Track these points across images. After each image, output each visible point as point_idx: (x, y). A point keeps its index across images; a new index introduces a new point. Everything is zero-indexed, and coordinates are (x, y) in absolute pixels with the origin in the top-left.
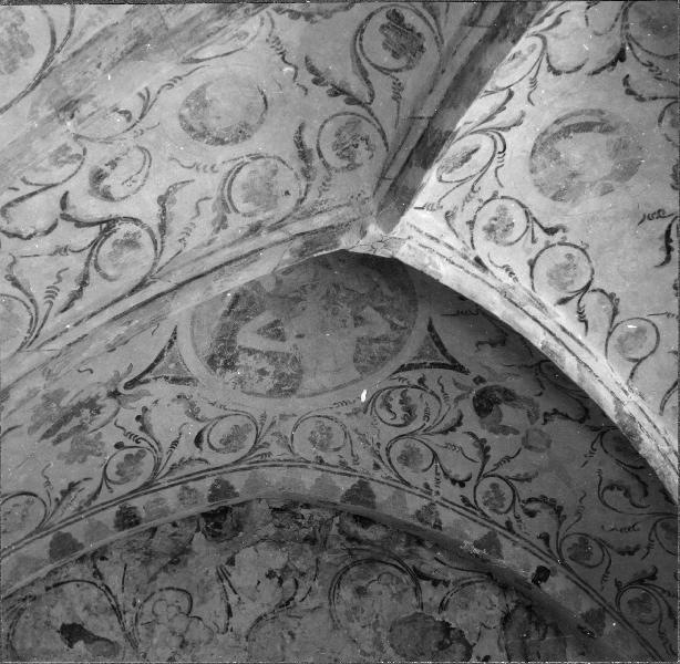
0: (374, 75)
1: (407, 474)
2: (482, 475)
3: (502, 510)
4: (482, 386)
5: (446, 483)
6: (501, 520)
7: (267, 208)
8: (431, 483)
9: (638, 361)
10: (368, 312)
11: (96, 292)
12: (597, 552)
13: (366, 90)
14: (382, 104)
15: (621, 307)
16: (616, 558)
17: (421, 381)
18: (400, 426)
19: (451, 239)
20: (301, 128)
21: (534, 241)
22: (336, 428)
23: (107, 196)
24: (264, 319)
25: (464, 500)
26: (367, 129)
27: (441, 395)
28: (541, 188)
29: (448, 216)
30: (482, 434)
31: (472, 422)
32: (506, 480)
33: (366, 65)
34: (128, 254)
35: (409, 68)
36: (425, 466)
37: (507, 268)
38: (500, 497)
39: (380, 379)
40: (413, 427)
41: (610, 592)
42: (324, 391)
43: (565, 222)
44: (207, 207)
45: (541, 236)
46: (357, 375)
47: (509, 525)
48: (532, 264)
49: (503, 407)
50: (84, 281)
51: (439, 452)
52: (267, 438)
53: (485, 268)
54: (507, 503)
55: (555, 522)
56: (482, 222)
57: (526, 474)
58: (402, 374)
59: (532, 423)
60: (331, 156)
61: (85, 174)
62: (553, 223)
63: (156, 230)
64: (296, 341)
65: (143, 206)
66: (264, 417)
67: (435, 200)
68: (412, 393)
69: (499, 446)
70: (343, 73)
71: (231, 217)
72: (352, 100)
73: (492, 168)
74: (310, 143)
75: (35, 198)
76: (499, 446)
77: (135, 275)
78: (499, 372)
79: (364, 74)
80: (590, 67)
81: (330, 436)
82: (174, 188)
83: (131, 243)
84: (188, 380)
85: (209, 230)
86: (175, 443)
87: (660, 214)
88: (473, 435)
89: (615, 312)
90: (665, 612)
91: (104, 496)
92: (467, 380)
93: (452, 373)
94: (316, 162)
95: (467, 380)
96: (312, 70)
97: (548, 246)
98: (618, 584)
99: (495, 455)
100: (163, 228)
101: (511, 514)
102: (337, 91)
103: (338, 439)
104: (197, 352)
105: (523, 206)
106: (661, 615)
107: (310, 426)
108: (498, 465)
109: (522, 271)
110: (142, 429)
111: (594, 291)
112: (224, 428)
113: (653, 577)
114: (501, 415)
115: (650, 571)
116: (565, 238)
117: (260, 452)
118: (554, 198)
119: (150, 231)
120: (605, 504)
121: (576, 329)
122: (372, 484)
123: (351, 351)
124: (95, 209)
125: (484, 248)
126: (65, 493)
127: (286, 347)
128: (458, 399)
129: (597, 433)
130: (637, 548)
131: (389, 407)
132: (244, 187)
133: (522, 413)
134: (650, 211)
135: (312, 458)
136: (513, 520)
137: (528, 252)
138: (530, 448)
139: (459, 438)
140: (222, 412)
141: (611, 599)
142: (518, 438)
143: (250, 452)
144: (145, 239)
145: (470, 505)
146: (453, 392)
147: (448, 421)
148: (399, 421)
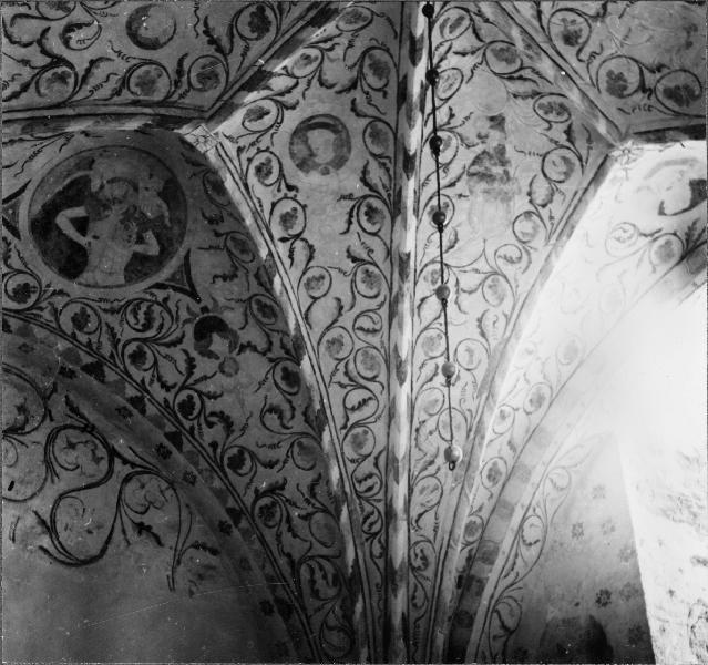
0: (237, 39)
1: (132, 370)
2: (183, 387)
3: (190, 417)
4: (206, 315)
5: (156, 385)
7: (146, 95)
8: (147, 381)
9: (315, 299)
10: (149, 236)
11: (24, 99)
12: (248, 463)
13: (228, 47)
14: (234, 60)
15: (315, 254)
16: (261, 469)
17: (166, 300)
18: (138, 331)
19: (236, 163)
20: (186, 55)
21: (279, 190)
23: (66, 43)
24: (79, 212)
26: (220, 69)
27: (175, 316)
28: (292, 155)
29: (240, 150)
30: (194, 354)
31: (189, 343)
32: (200, 394)
33: (235, 32)
34: (57, 86)
35: (257, 39)
36: (147, 366)
37: (260, 201)
38: (192, 406)
39: (137, 290)
40: (150, 334)
41: (249, 498)
42: (96, 286)
43: (299, 185)
44: (114, 79)
45: (283, 186)
46: (122, 281)
48: (274, 205)
49: (216, 337)
50: (25, 88)
51: (160, 359)
52: (44, 305)
53: (249, 193)
54: (195, 413)
55: (224, 436)
56: (256, 163)
57: (215, 393)
58: (155, 291)
59: (231, 352)
60: (194, 80)
61: (64, 23)
62: (292, 182)
63: (80, 79)
64: (92, 240)
65: (80, 61)
66: (48, 286)
67: (235, 137)
68: (157, 309)
69: (204, 366)
70: (220, 31)
71: (125, 91)
72: (220, 49)
73: (272, 131)
74: (186, 66)
75: (33, 21)
76: (204, 366)
77: (55, 98)
78: (221, 305)
79: (231, 36)
80: (337, 88)
81: (87, 321)
82: (100, 59)
83: (62, 78)
84: (16, 233)
85: (109, 92)
87: (350, 197)
89: (311, 258)
90: (284, 519)
92: (196, 308)
93: (187, 300)
94: (185, 79)
95: (196, 308)
96: (206, 24)
97: (286, 197)
98: (256, 491)
99: (198, 373)
100: (85, 79)
101: (195, 422)
102: (212, 41)
103: (92, 325)
104: (29, 212)
105: (280, 163)
106: (281, 520)
107: (76, 308)
108: (196, 382)
109: (267, 207)
111: (303, 240)
113: (282, 488)
114: (211, 341)
115: (281, 482)
116: (295, 196)
117: (34, 311)
118: (297, 166)
119: (76, 75)
120: (264, 425)
121: (287, 262)
122: (106, 369)
123: (126, 260)
124: (55, 44)
125: (252, 180)
127: (83, 241)
128: (186, 322)
129: (273, 364)
130: (277, 462)
131: (136, 317)
132: (139, 77)
133: (227, 343)
134: (347, 193)
135: (69, 333)
136: (197, 427)
137: (274, 196)
138: (223, 372)
139: (176, 353)
140: (23, 268)
141: (249, 504)
142: (217, 363)
143: (28, 309)
144: (71, 81)
145: (168, 406)
146: (184, 315)
148: (139, 327)
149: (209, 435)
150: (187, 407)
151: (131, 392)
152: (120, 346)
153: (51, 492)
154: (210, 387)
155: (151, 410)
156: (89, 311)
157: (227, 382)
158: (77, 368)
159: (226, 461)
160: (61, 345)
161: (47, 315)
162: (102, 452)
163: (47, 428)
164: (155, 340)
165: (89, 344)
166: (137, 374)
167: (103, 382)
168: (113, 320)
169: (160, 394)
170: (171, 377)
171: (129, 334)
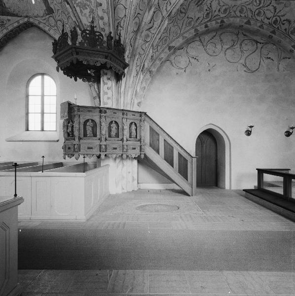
1: (259, 18)
5: (266, 19)
6: (276, 27)
22: (245, 8)
25: (269, 23)
40: (261, 5)
47: (278, 29)
51: (266, 12)
76: (279, 8)
86: (215, 11)
88: (273, 6)
91: (203, 22)
99: (277, 11)
107: (239, 8)
110: (210, 6)
112: (224, 8)
126: (197, 20)
139: (271, 8)
142: (283, 4)
147: (268, 3)
149: (283, 27)
150: (276, 22)
151: (259, 24)
152: (253, 13)
153: (244, 58)
154: (282, 13)
155: (265, 26)
156: (243, 7)
157: (288, 9)
158: (243, 24)
159: (290, 33)
160: (238, 20)
161: (233, 13)
162: (254, 43)
163: (239, 43)
164: (263, 7)
165: (245, 16)
166: (259, 18)
167: (251, 25)
168: (249, 7)
169: (266, 21)
170: (269, 15)
171: (256, 8)
